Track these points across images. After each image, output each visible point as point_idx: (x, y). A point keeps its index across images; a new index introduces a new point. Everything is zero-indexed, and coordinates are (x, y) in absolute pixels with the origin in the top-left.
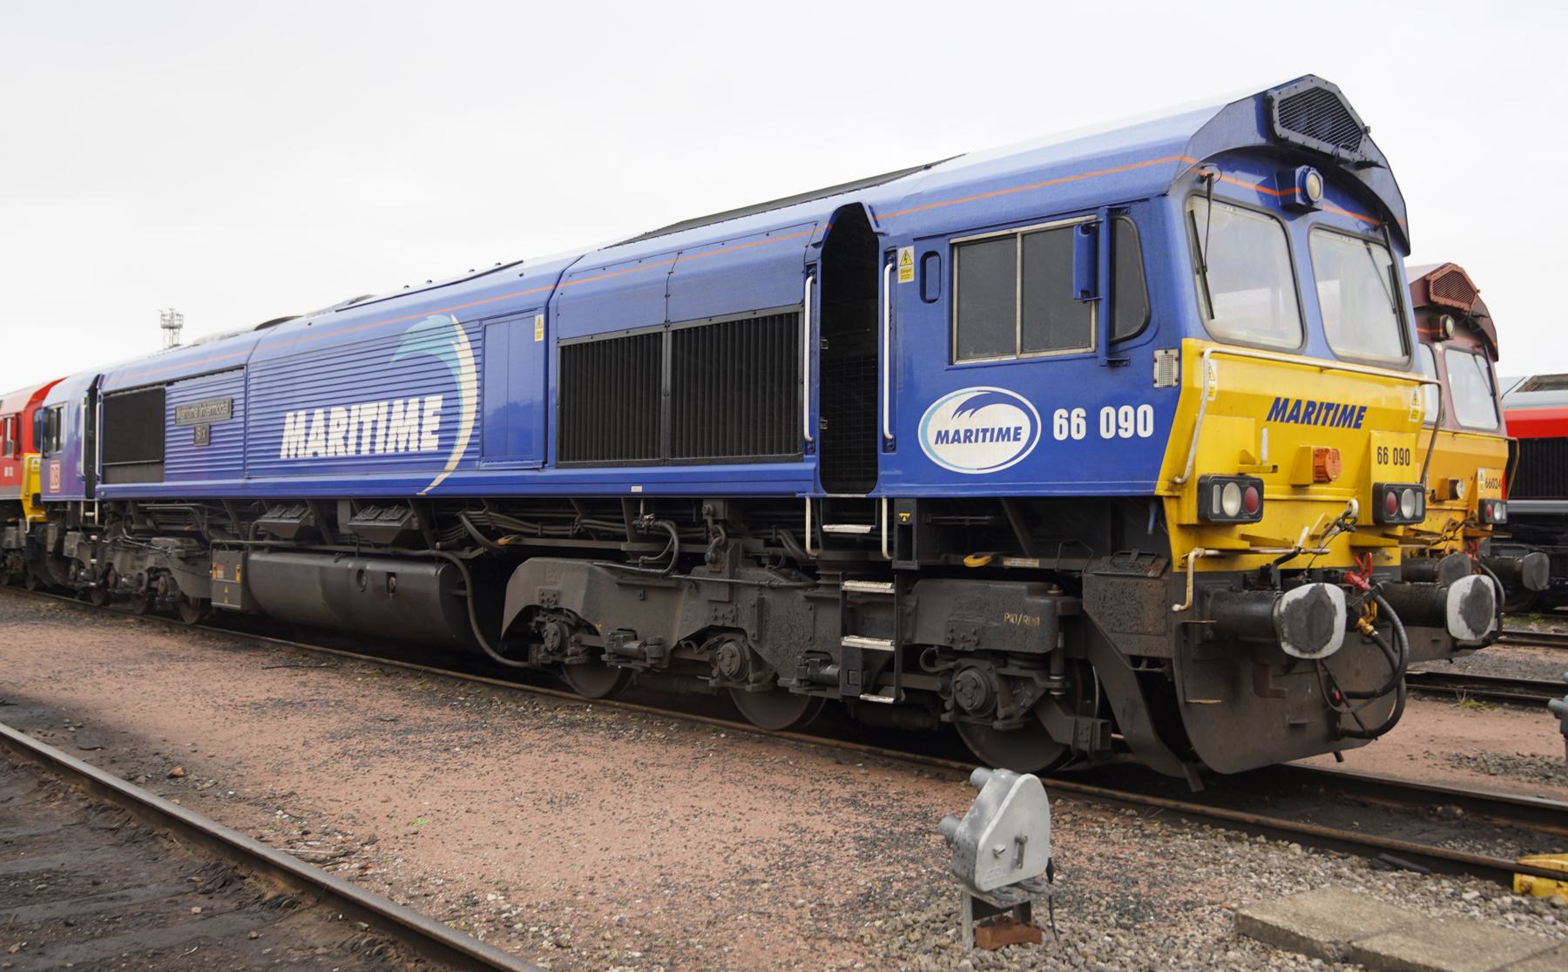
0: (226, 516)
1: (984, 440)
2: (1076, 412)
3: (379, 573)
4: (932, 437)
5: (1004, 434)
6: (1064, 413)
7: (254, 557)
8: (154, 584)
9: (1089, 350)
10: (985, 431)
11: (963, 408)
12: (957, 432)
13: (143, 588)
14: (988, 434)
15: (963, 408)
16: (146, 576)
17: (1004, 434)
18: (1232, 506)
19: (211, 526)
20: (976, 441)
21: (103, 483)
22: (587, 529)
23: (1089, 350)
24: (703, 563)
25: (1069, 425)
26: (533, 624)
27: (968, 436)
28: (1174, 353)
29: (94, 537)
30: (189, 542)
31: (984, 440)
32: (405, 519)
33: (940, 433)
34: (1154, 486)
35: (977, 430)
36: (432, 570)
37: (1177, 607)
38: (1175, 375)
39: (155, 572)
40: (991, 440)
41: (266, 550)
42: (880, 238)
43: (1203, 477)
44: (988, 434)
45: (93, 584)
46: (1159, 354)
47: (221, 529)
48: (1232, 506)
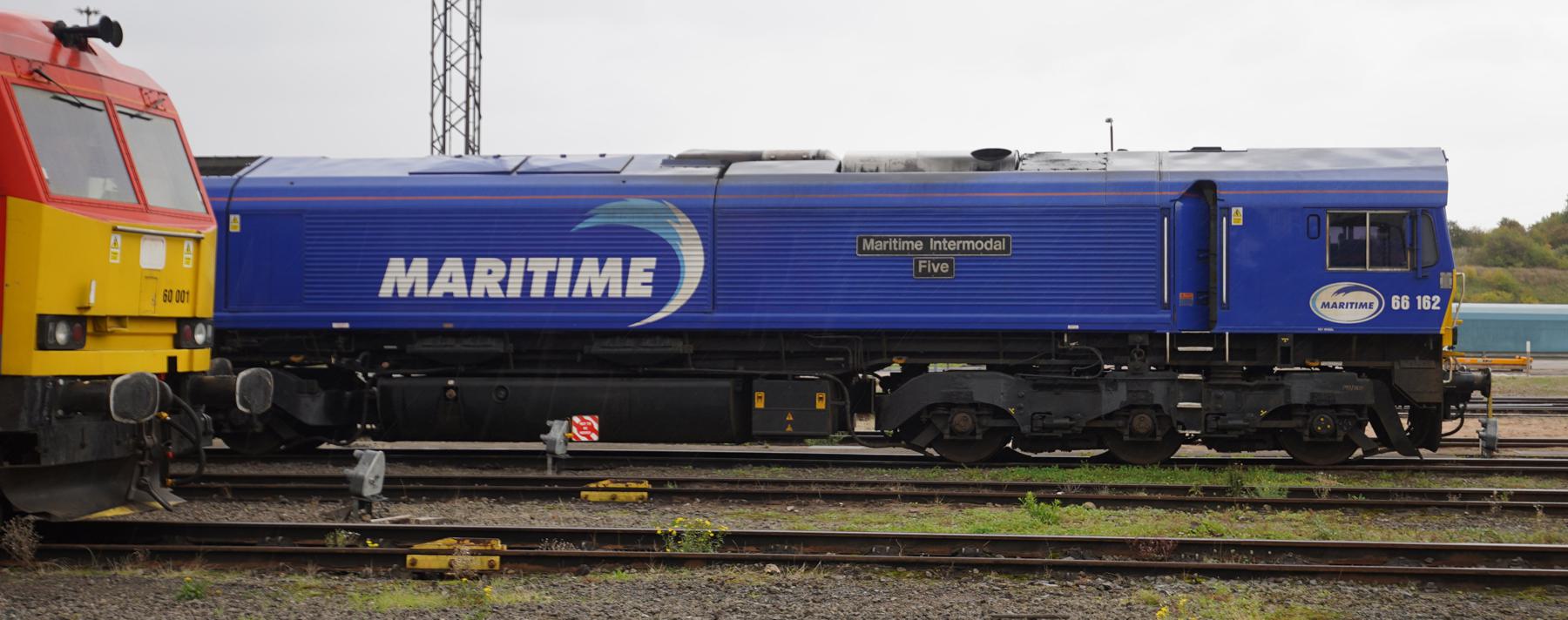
1: (1351, 307)
2: (1403, 297)
4: (1319, 305)
5: (1363, 305)
6: (1398, 297)
9: (1404, 270)
10: (1352, 304)
11: (1339, 292)
12: (1335, 303)
14: (1354, 306)
15: (1339, 292)
17: (1363, 305)
20: (1347, 307)
23: (1404, 270)
25: (1400, 303)
27: (1341, 305)
28: (1450, 274)
31: (1351, 307)
33: (1324, 303)
34: (1439, 330)
35: (1347, 304)
36: (727, 383)
37: (1445, 382)
38: (1450, 283)
40: (1356, 307)
44: (1354, 306)
46: (1442, 274)
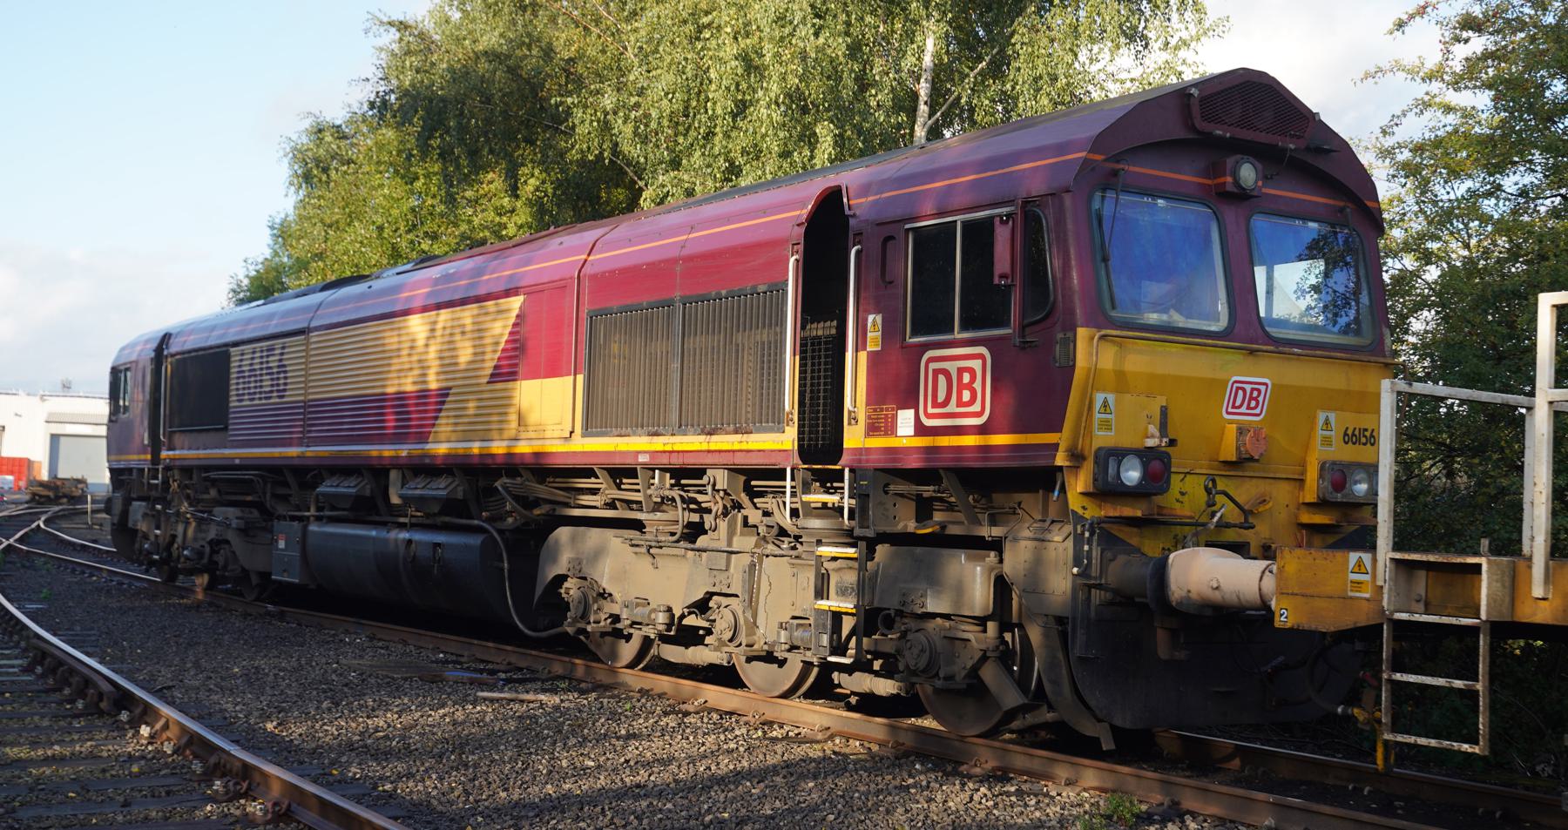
0: (286, 485)
3: (426, 544)
7: (313, 528)
8: (216, 558)
13: (205, 561)
16: (208, 549)
18: (1132, 475)
19: (274, 496)
21: (170, 449)
22: (614, 499)
24: (705, 532)
26: (562, 591)
29: (159, 507)
30: (251, 513)
32: (450, 488)
39: (216, 544)
41: (324, 521)
42: (852, 222)
43: (1100, 449)
45: (156, 557)
47: (285, 499)
48: (1132, 475)
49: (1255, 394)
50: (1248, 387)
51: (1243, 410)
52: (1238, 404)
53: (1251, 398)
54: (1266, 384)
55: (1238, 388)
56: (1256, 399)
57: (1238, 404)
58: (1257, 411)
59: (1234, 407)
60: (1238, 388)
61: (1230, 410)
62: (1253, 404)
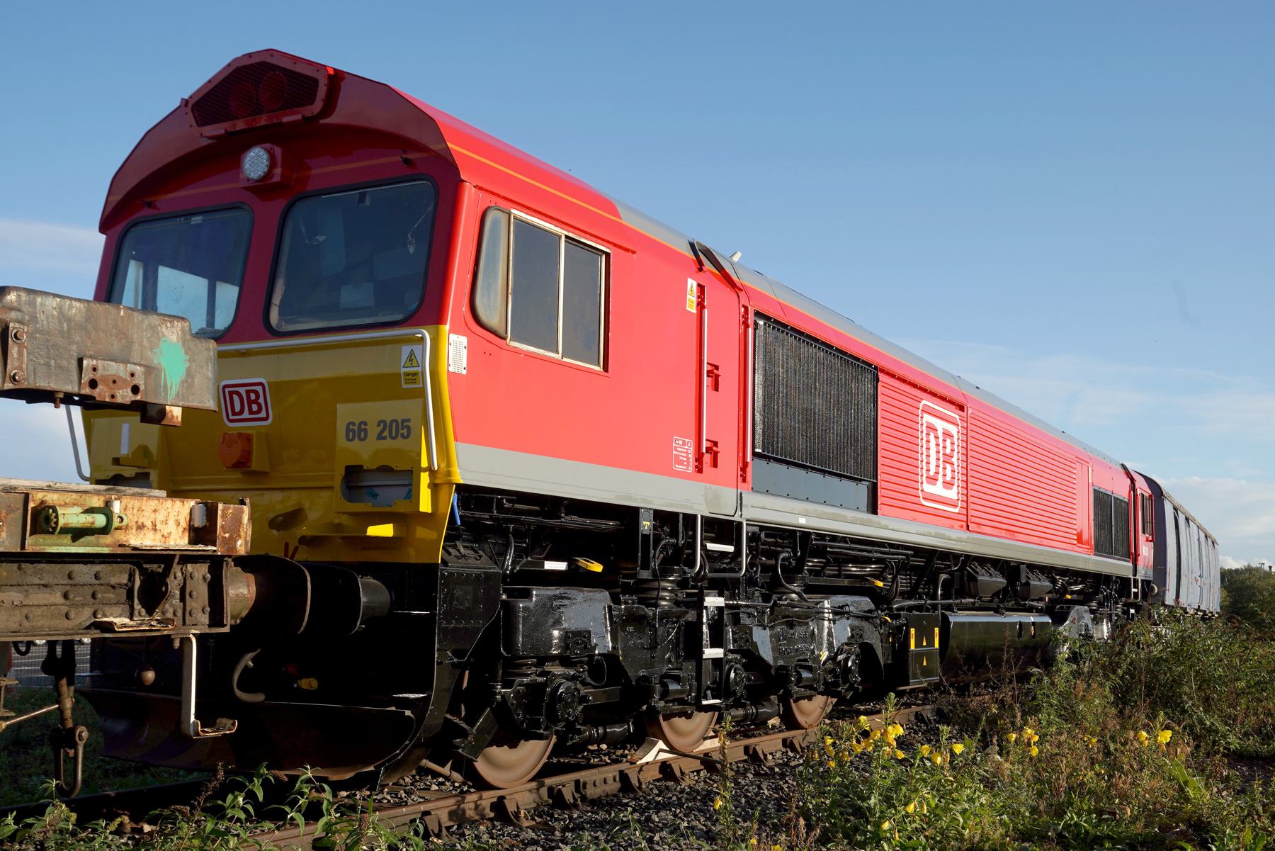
49: (253, 396)
50: (242, 390)
51: (246, 415)
52: (237, 409)
53: (250, 402)
54: (261, 384)
55: (231, 393)
56: (256, 401)
57: (237, 409)
58: (263, 414)
59: (234, 413)
60: (231, 393)
61: (231, 417)
62: (255, 407)
